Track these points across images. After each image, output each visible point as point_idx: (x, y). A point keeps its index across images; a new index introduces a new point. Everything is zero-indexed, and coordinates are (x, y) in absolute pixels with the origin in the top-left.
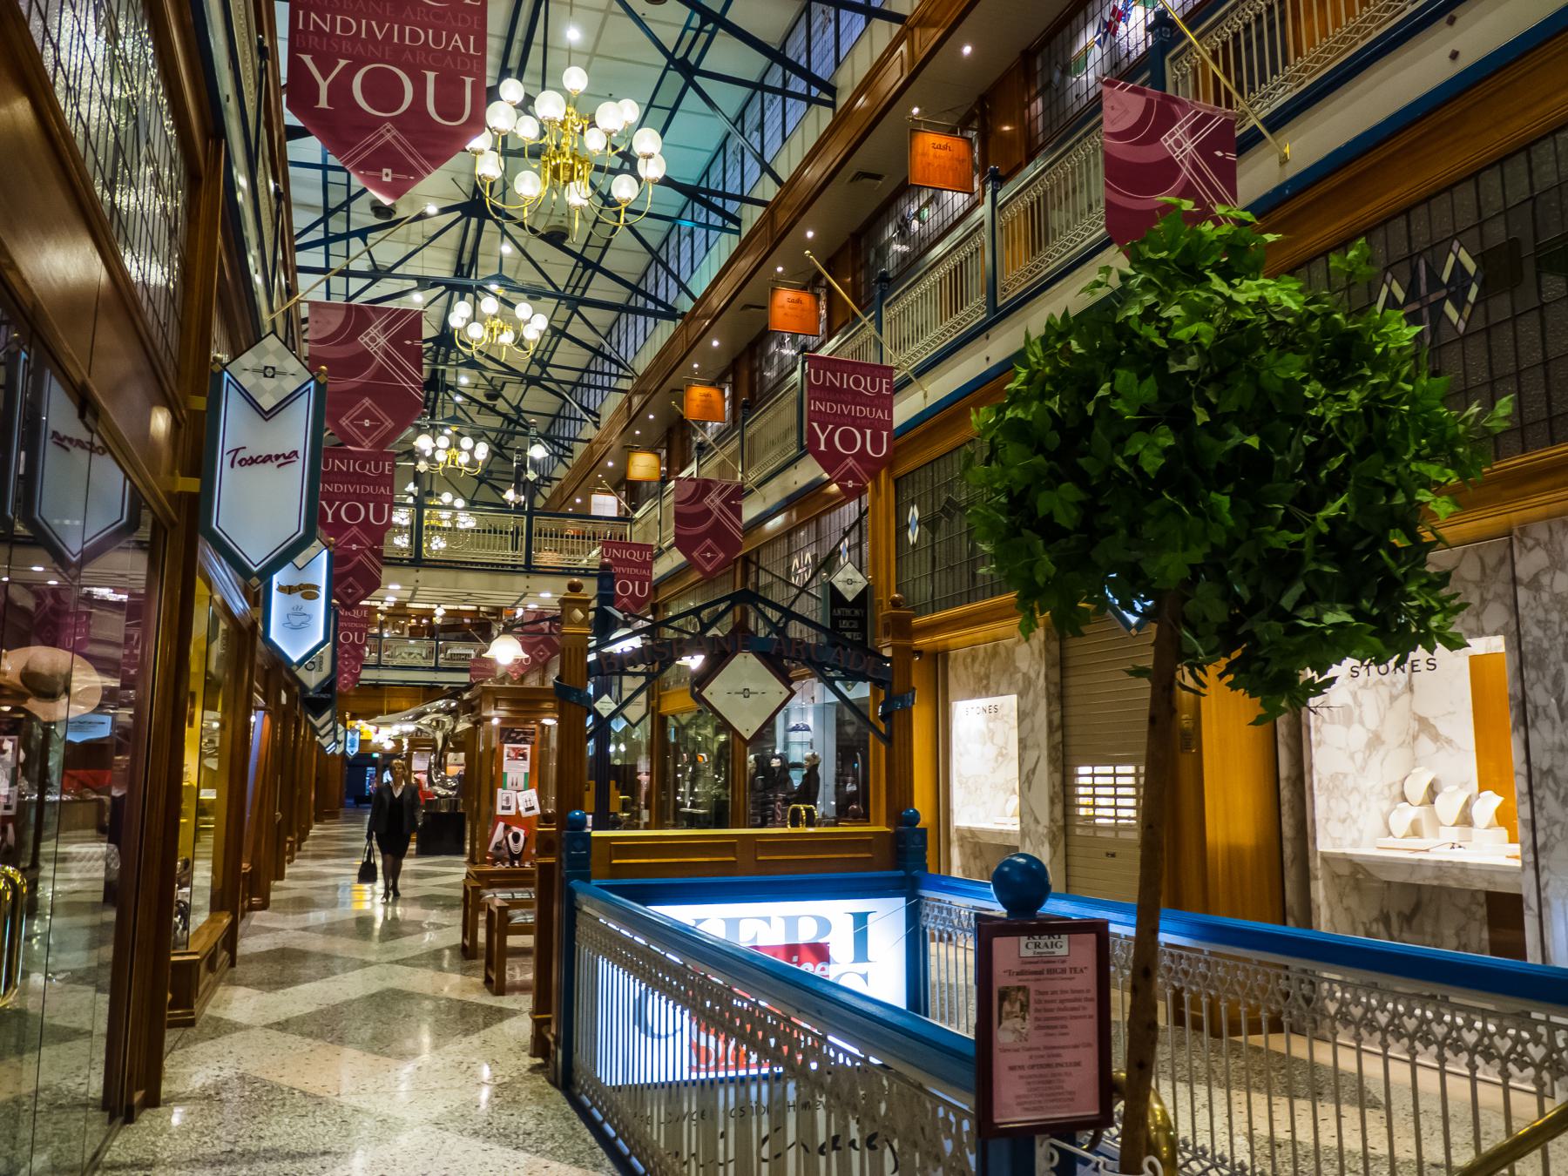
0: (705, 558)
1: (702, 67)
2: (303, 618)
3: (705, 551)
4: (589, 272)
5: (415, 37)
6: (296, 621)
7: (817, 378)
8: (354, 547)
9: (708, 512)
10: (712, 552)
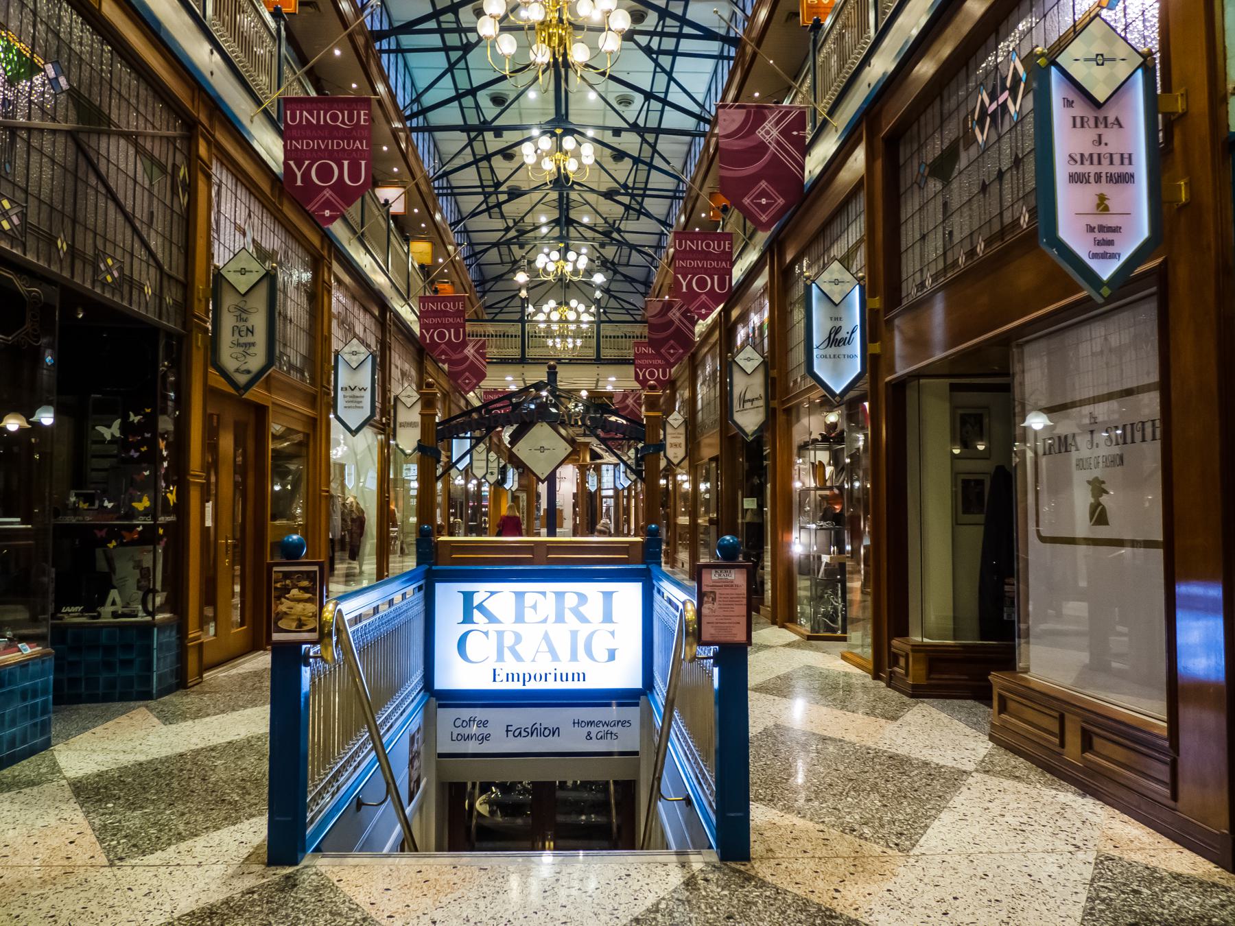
5: (338, 145)
9: (672, 322)
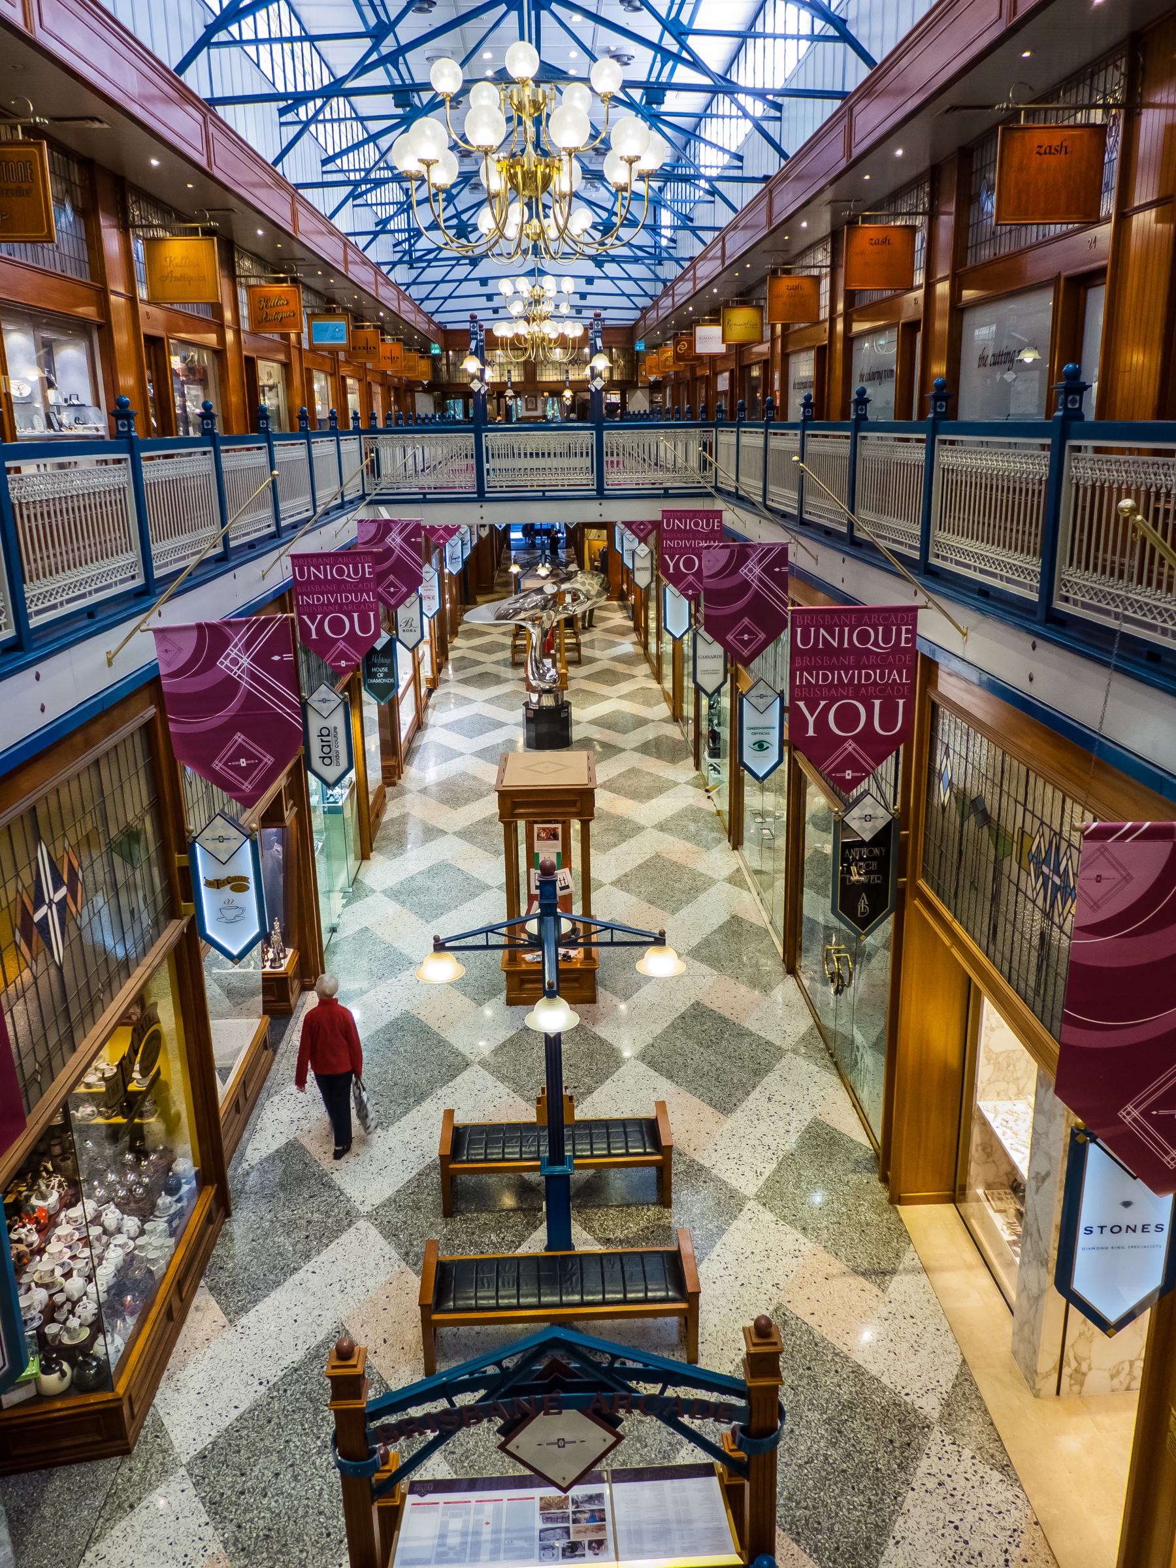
0: (742, 642)
1: (695, 26)
2: (236, 912)
3: (742, 633)
4: (670, 63)
6: (230, 914)
7: (805, 640)
8: (343, 664)
9: (746, 585)
10: (751, 633)
